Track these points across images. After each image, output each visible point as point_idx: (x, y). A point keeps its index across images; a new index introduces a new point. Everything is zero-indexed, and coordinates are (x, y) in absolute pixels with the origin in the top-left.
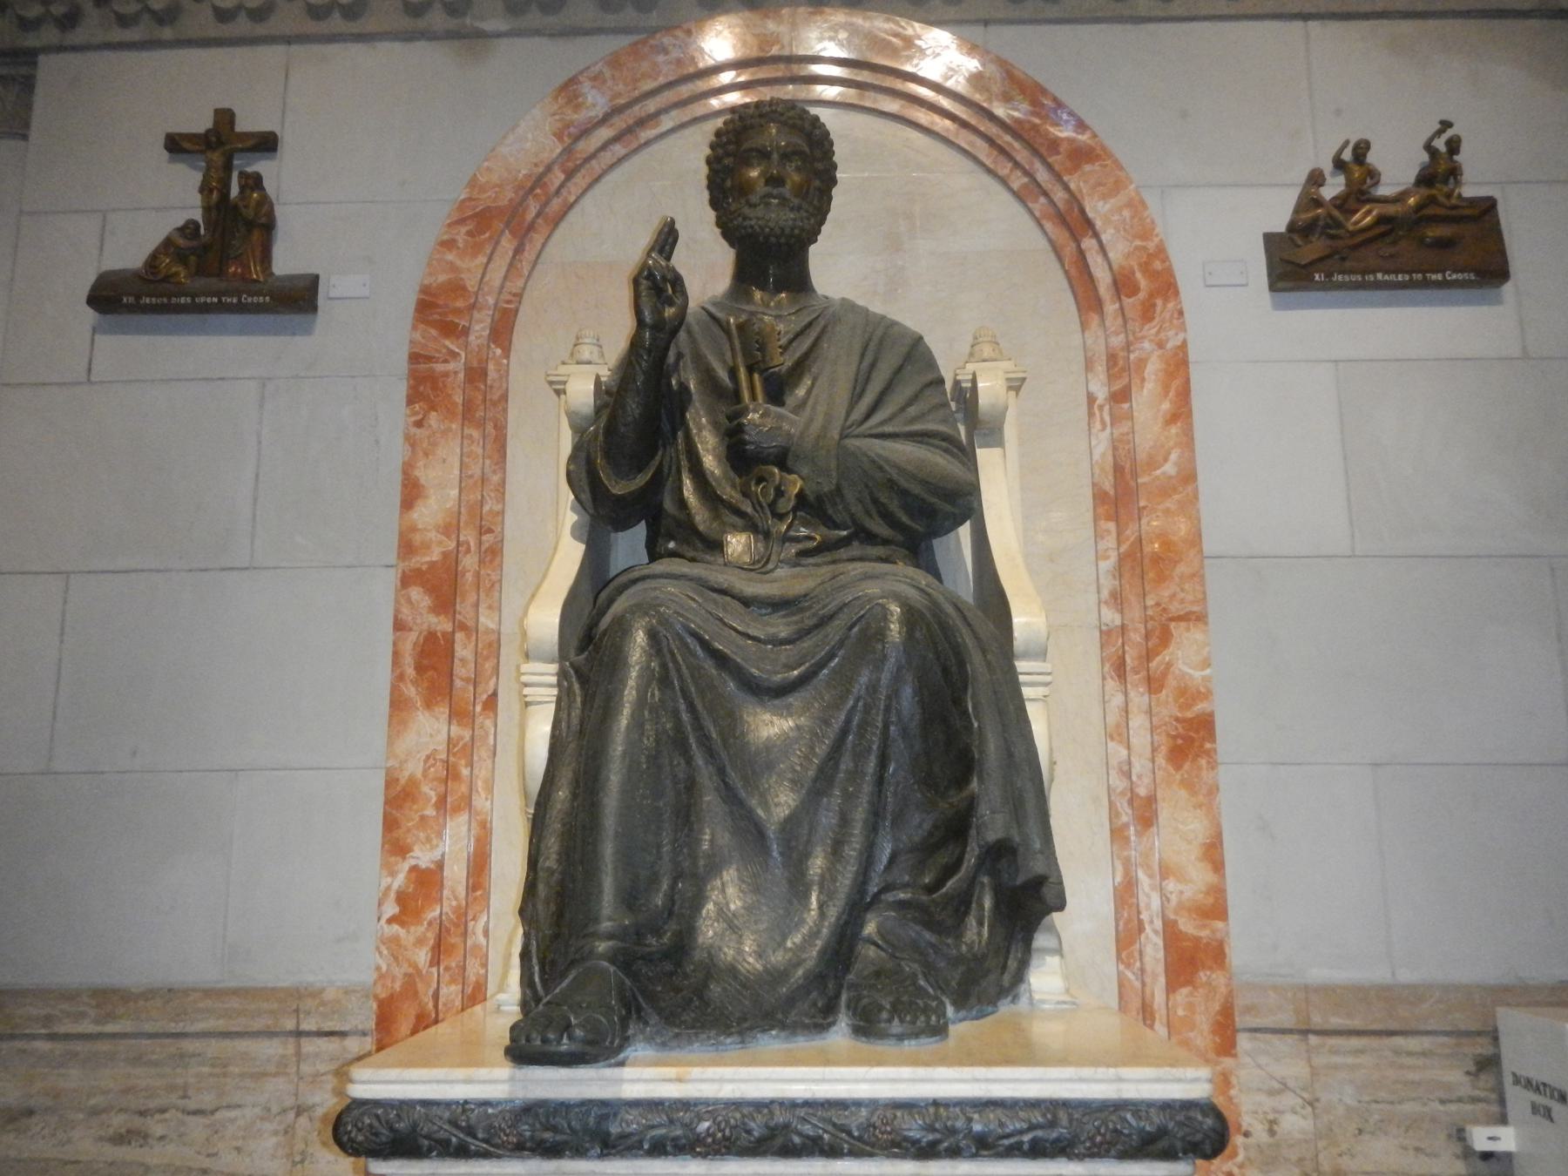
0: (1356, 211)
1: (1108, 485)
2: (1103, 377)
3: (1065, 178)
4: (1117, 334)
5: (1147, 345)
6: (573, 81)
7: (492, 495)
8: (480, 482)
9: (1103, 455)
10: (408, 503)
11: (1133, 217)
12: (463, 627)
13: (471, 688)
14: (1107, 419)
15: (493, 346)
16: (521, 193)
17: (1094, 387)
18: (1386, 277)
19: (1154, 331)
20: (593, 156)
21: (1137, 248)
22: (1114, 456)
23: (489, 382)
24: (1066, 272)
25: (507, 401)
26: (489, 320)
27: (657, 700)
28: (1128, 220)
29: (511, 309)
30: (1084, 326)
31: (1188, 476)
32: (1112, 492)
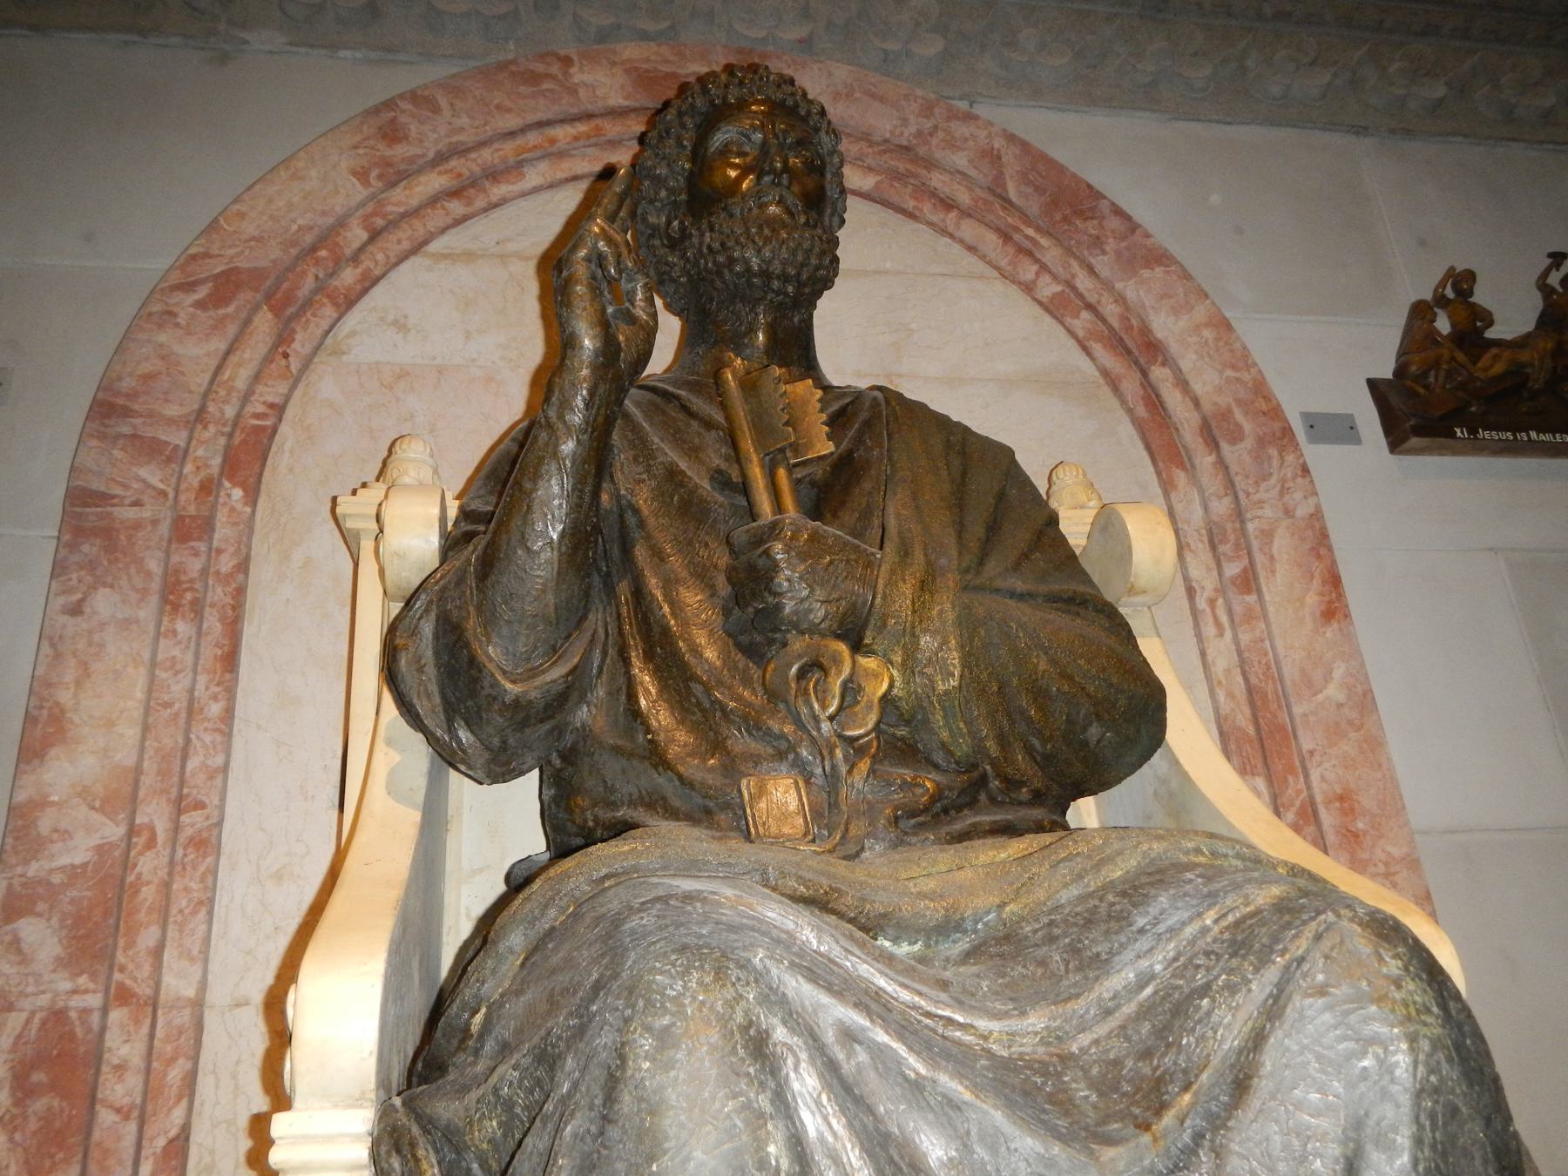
0: (1479, 357)
1: (1243, 719)
2: (1205, 555)
3: (1119, 286)
4: (1220, 498)
5: (1268, 512)
6: (389, 104)
7: (208, 738)
8: (183, 715)
9: (1228, 671)
10: (31, 752)
11: (1217, 340)
12: (124, 996)
13: (131, 1128)
14: (1224, 619)
15: (227, 484)
16: (294, 251)
17: (1195, 572)
18: (1542, 437)
19: (1275, 492)
20: (414, 213)
21: (1228, 381)
22: (1244, 674)
23: (215, 544)
25: (246, 573)
26: (222, 441)
28: (1211, 341)
29: (263, 428)
30: (1167, 486)
31: (1365, 701)
32: (1251, 731)
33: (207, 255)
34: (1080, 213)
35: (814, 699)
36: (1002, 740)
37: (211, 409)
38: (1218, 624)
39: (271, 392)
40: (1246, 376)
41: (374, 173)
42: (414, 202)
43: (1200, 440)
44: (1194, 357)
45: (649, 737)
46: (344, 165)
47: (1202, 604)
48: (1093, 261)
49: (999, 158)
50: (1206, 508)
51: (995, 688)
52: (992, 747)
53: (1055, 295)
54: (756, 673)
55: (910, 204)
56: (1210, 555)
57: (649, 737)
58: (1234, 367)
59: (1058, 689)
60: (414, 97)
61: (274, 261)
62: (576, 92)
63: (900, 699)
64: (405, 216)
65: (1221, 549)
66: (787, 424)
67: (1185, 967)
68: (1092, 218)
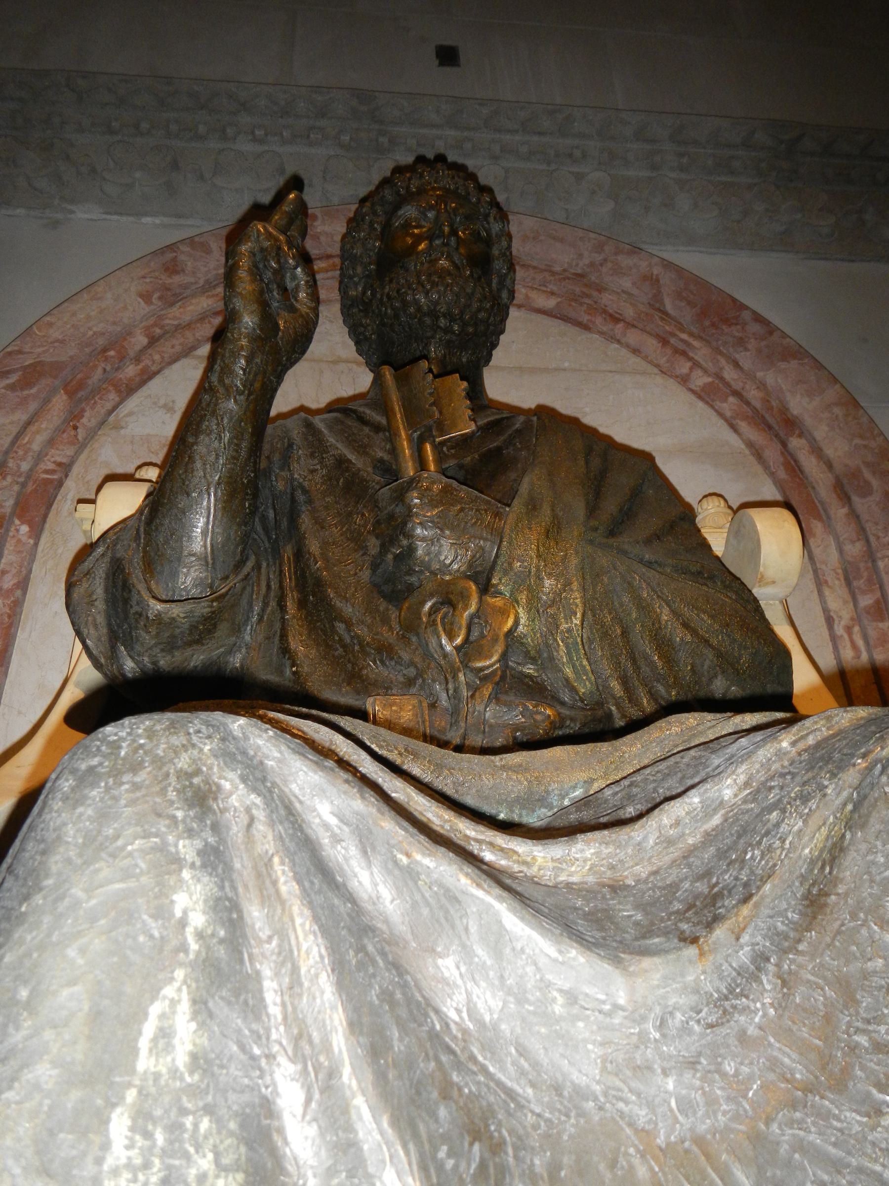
2: (843, 591)
3: (760, 374)
6: (171, 247)
14: (860, 643)
15: (17, 522)
16: (87, 350)
17: (834, 604)
24: (772, 475)
26: (16, 488)
27: (181, 1059)
33: (20, 352)
34: (727, 321)
35: (440, 629)
36: (624, 681)
37: (10, 465)
38: (854, 646)
39: (61, 454)
40: (873, 444)
41: (156, 295)
42: (187, 318)
43: (834, 495)
44: (826, 429)
45: (294, 669)
46: (133, 289)
47: (840, 630)
48: (737, 356)
49: (658, 280)
50: (841, 551)
51: (619, 631)
52: (616, 686)
53: (706, 385)
54: (394, 614)
55: (585, 318)
56: (846, 590)
57: (294, 669)
58: (861, 437)
59: (681, 639)
60: (191, 241)
61: (71, 357)
62: (318, 238)
63: (525, 636)
64: (177, 327)
65: (855, 584)
66: (433, 404)
67: (758, 791)
68: (737, 324)
